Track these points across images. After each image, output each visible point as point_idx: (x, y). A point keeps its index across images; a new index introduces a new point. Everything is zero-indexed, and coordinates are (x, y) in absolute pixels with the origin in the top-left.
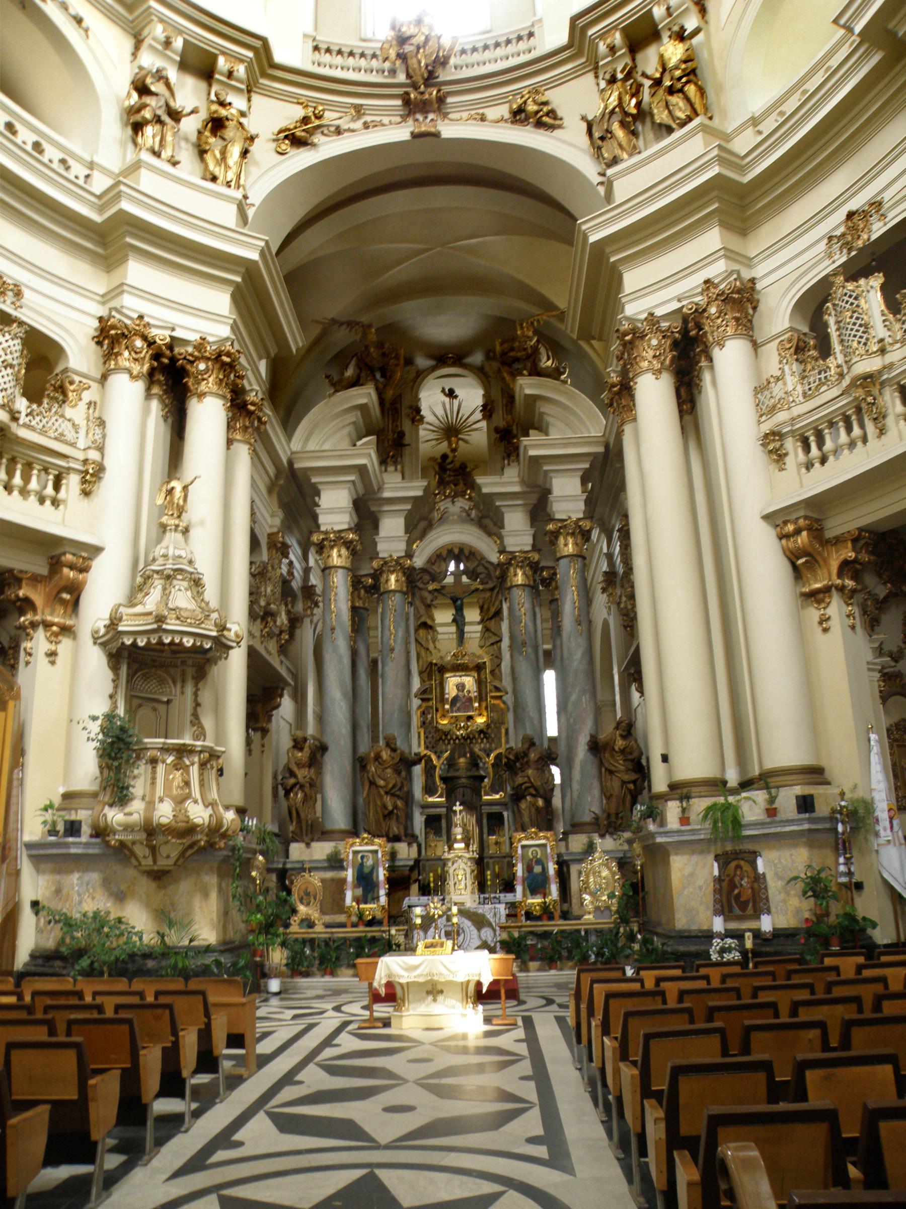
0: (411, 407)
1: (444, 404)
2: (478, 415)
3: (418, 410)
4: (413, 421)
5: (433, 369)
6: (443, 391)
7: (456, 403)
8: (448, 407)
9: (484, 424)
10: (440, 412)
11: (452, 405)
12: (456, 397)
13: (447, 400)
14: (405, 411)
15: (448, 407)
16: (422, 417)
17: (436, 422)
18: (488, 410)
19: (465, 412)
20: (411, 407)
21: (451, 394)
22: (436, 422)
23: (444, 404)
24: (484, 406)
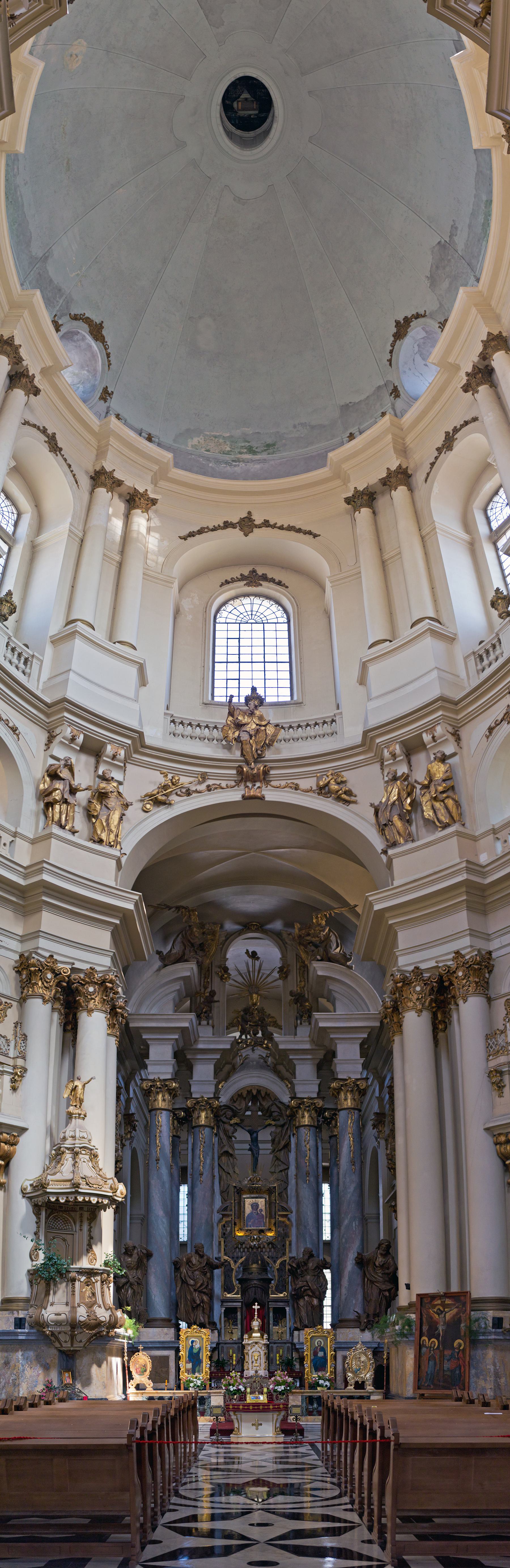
0: (220, 967)
1: (247, 964)
2: (276, 975)
3: (226, 970)
4: (222, 978)
5: (239, 933)
7: (257, 963)
9: (280, 982)
11: (254, 965)
12: (258, 958)
13: (250, 961)
14: (215, 969)
16: (229, 975)
17: (240, 979)
18: (284, 971)
20: (220, 967)
21: (254, 955)
22: (240, 979)
23: (247, 964)
24: (281, 970)
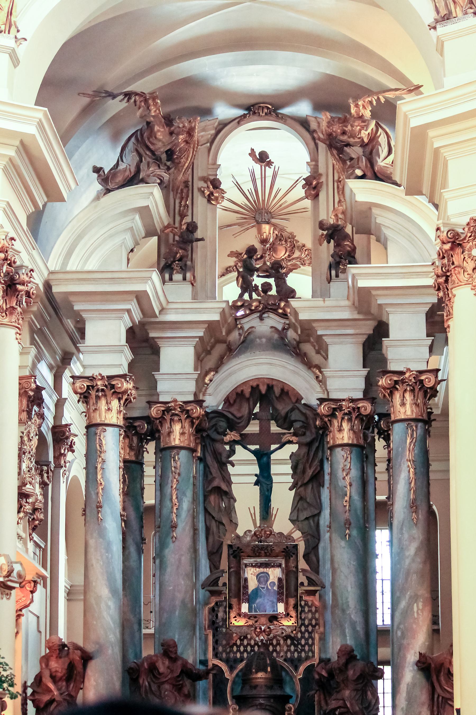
0: (205, 179)
2: (300, 192)
3: (216, 184)
4: (209, 199)
5: (240, 120)
6: (252, 153)
7: (269, 172)
8: (258, 176)
9: (308, 203)
10: (248, 186)
11: (263, 178)
12: (270, 164)
13: (257, 167)
14: (199, 184)
15: (258, 176)
16: (223, 191)
17: (241, 199)
18: (313, 186)
19: (282, 184)
20: (205, 179)
21: (263, 159)
22: (241, 199)
24: (308, 182)
